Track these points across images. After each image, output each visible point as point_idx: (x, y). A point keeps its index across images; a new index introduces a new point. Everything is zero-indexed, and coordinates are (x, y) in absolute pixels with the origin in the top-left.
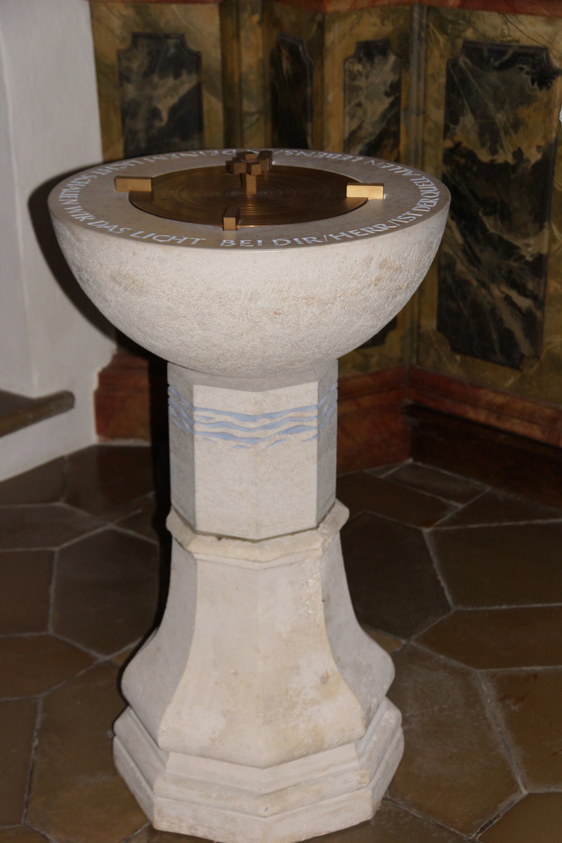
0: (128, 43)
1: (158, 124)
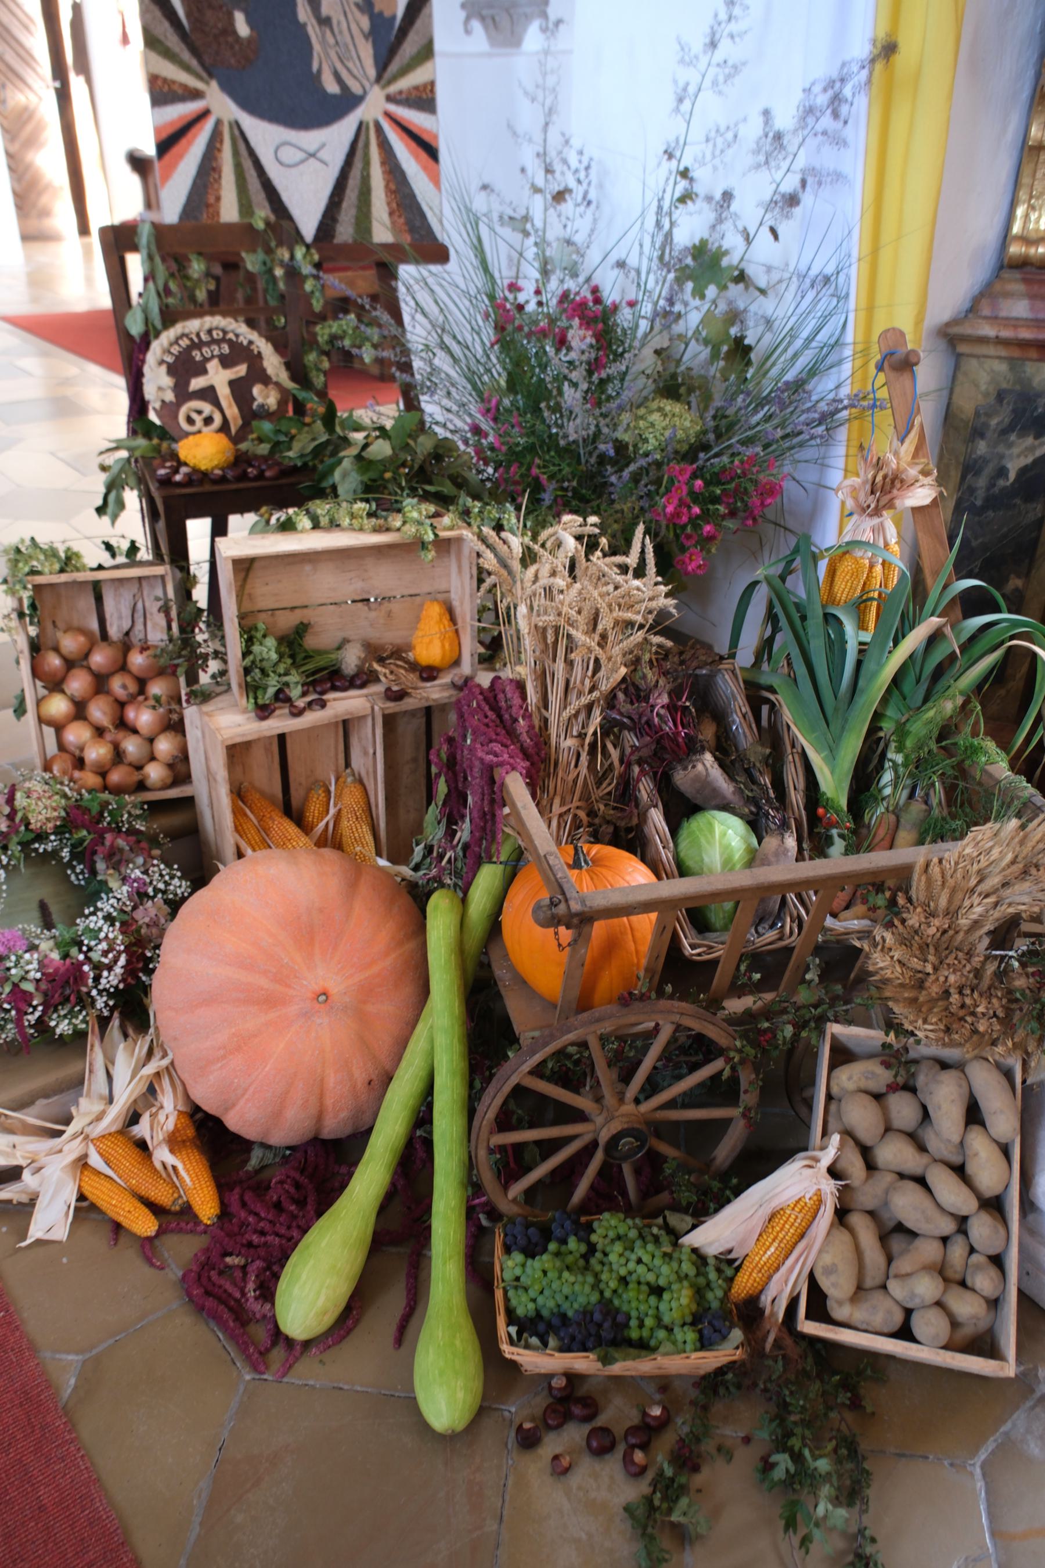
0: (992, 400)
1: (1001, 483)
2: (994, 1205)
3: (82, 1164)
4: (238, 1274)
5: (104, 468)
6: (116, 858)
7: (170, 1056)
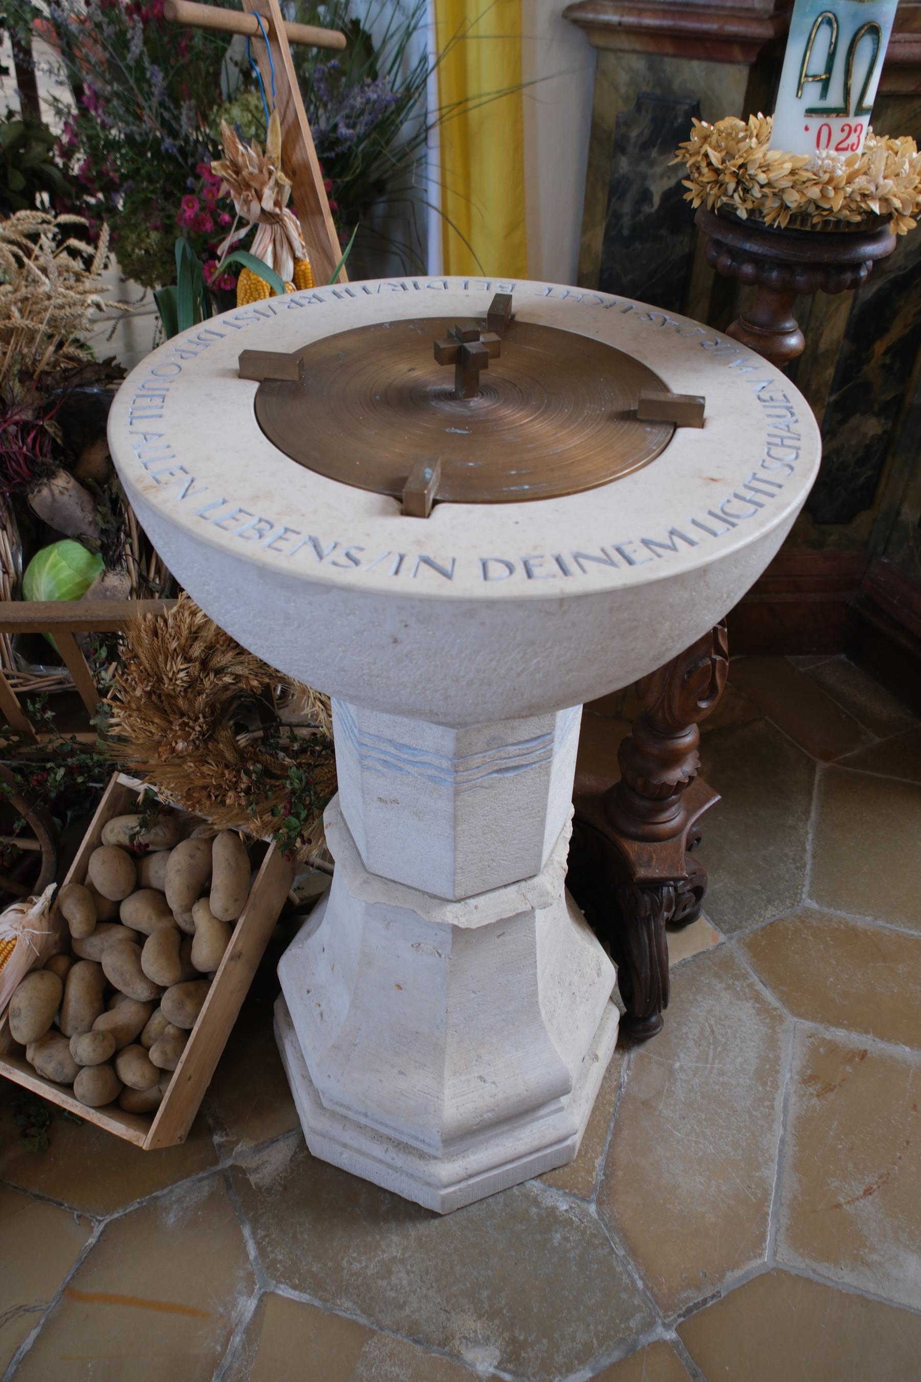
1: (646, 209)
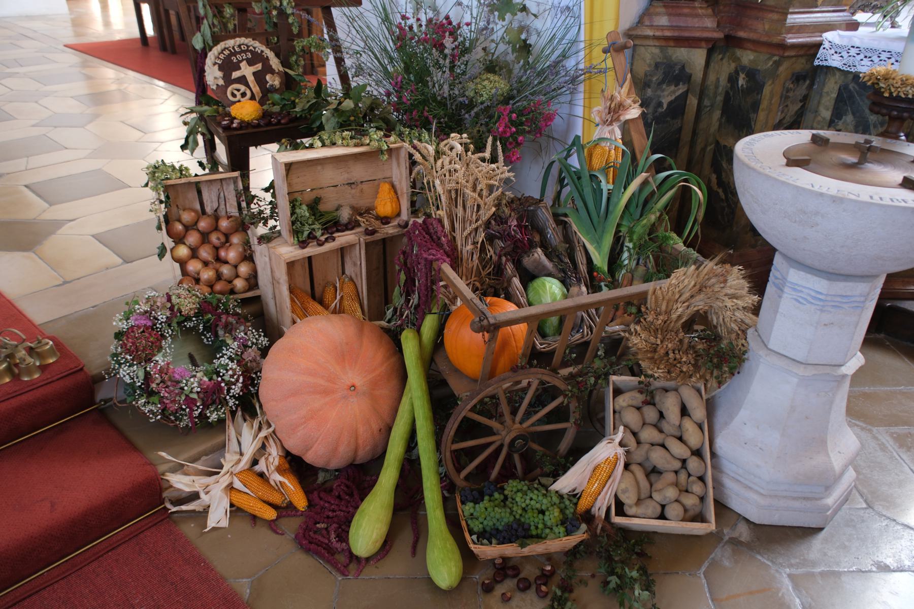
1: (660, 110)
2: (698, 453)
3: (230, 488)
4: (324, 532)
5: (185, 123)
6: (230, 327)
7: (273, 426)
